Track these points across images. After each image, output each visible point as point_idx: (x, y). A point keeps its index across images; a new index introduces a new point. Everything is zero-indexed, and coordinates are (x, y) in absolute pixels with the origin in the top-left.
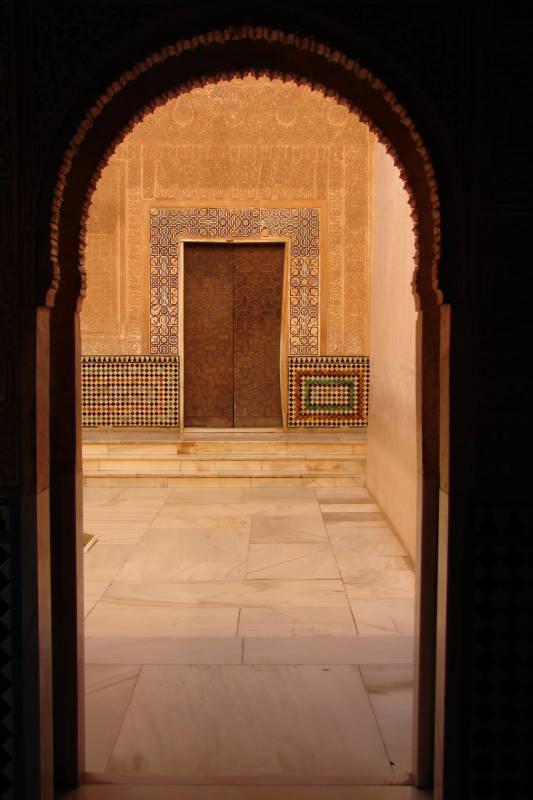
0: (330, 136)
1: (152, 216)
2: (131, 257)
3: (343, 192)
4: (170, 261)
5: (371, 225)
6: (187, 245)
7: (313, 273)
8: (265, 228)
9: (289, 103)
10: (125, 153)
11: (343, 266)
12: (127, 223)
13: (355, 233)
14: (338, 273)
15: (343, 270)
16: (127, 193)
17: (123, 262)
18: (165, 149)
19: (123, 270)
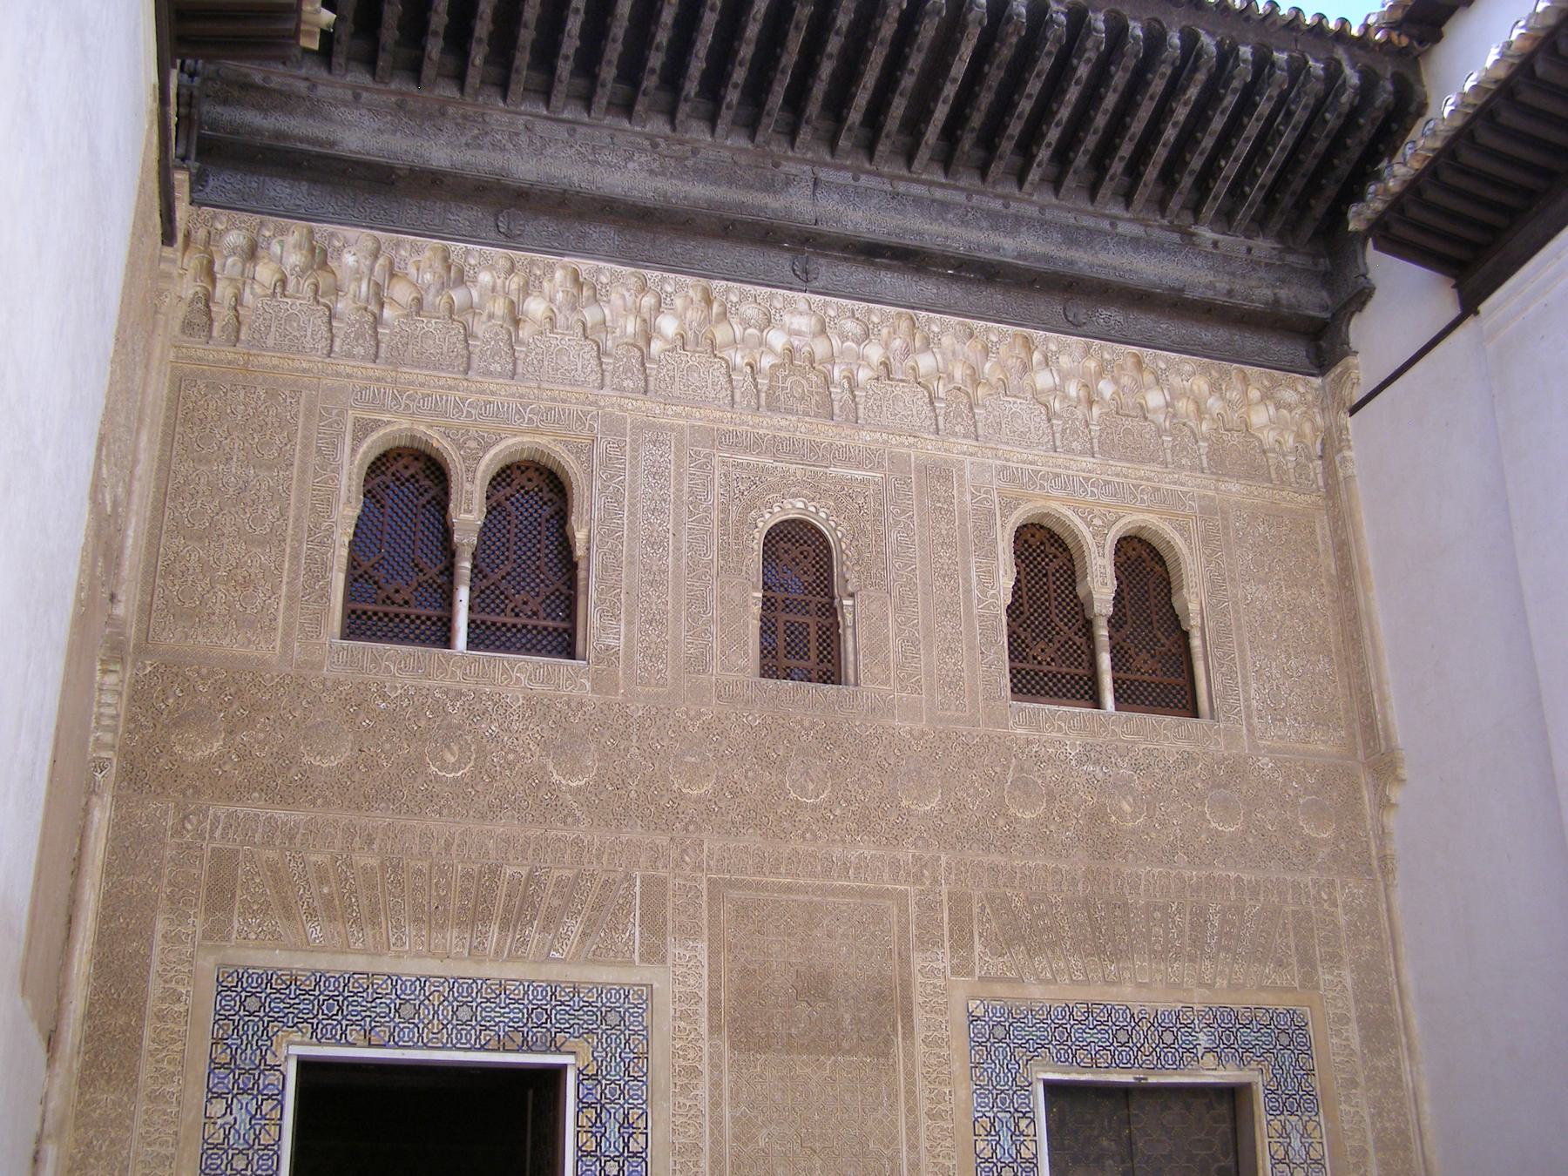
0: (1310, 856)
1: (973, 1019)
2: (931, 1115)
3: (1348, 978)
4: (1017, 1125)
5: (1410, 1048)
6: (1052, 1088)
7: (1313, 1154)
8: (1210, 1050)
9: (1225, 786)
10: (908, 874)
11: (1370, 1137)
12: (920, 1033)
13: (1381, 1063)
14: (1362, 1153)
15: (1371, 1150)
16: (917, 961)
17: (913, 1128)
18: (993, 869)
19: (913, 1147)
